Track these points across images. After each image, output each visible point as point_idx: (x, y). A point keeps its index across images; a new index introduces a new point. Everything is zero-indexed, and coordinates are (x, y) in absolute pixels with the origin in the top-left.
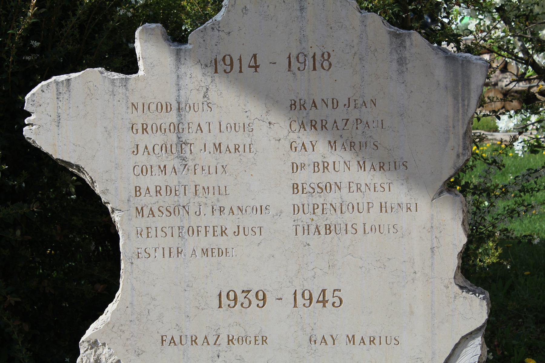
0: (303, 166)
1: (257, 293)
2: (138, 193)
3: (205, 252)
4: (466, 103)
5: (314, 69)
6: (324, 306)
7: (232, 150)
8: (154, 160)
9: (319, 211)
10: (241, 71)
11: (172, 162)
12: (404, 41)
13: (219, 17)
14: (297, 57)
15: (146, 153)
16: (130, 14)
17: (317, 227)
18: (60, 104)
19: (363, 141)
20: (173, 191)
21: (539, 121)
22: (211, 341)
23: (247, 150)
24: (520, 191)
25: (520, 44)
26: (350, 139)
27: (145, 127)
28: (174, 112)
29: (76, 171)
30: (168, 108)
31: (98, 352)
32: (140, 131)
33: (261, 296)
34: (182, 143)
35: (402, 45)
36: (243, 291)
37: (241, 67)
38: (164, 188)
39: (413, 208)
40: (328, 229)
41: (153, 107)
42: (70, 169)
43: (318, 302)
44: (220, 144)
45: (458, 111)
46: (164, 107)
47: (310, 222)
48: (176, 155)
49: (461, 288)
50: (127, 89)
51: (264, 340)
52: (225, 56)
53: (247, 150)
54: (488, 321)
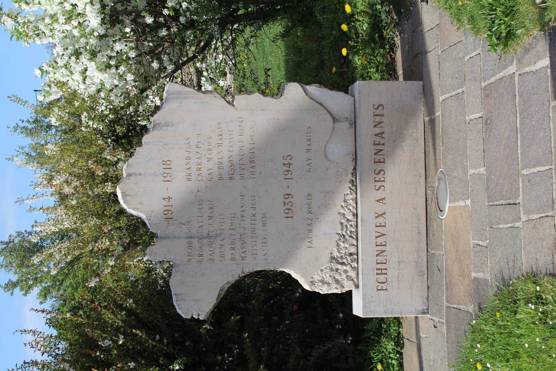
1: (285, 198)
2: (234, 259)
3: (264, 225)
4: (188, 93)
5: (171, 168)
6: (292, 164)
7: (212, 210)
8: (217, 251)
9: (243, 167)
10: (172, 206)
11: (218, 242)
12: (157, 123)
14: (165, 177)
15: (213, 255)
17: (251, 167)
19: (207, 144)
20: (233, 241)
21: (207, 70)
22: (310, 222)
23: (212, 203)
24: (244, 78)
25: (161, 80)
27: (200, 255)
28: (192, 240)
30: (190, 243)
32: (202, 258)
33: (287, 196)
34: (208, 236)
35: (159, 124)
36: (285, 205)
37: (170, 206)
38: (232, 246)
39: (241, 119)
40: (252, 162)
41: (190, 251)
43: (289, 167)
44: (209, 217)
46: (190, 245)
47: (249, 171)
49: (281, 96)
50: (180, 265)
51: (310, 195)
52: (164, 214)
53: (212, 203)
54: (298, 82)
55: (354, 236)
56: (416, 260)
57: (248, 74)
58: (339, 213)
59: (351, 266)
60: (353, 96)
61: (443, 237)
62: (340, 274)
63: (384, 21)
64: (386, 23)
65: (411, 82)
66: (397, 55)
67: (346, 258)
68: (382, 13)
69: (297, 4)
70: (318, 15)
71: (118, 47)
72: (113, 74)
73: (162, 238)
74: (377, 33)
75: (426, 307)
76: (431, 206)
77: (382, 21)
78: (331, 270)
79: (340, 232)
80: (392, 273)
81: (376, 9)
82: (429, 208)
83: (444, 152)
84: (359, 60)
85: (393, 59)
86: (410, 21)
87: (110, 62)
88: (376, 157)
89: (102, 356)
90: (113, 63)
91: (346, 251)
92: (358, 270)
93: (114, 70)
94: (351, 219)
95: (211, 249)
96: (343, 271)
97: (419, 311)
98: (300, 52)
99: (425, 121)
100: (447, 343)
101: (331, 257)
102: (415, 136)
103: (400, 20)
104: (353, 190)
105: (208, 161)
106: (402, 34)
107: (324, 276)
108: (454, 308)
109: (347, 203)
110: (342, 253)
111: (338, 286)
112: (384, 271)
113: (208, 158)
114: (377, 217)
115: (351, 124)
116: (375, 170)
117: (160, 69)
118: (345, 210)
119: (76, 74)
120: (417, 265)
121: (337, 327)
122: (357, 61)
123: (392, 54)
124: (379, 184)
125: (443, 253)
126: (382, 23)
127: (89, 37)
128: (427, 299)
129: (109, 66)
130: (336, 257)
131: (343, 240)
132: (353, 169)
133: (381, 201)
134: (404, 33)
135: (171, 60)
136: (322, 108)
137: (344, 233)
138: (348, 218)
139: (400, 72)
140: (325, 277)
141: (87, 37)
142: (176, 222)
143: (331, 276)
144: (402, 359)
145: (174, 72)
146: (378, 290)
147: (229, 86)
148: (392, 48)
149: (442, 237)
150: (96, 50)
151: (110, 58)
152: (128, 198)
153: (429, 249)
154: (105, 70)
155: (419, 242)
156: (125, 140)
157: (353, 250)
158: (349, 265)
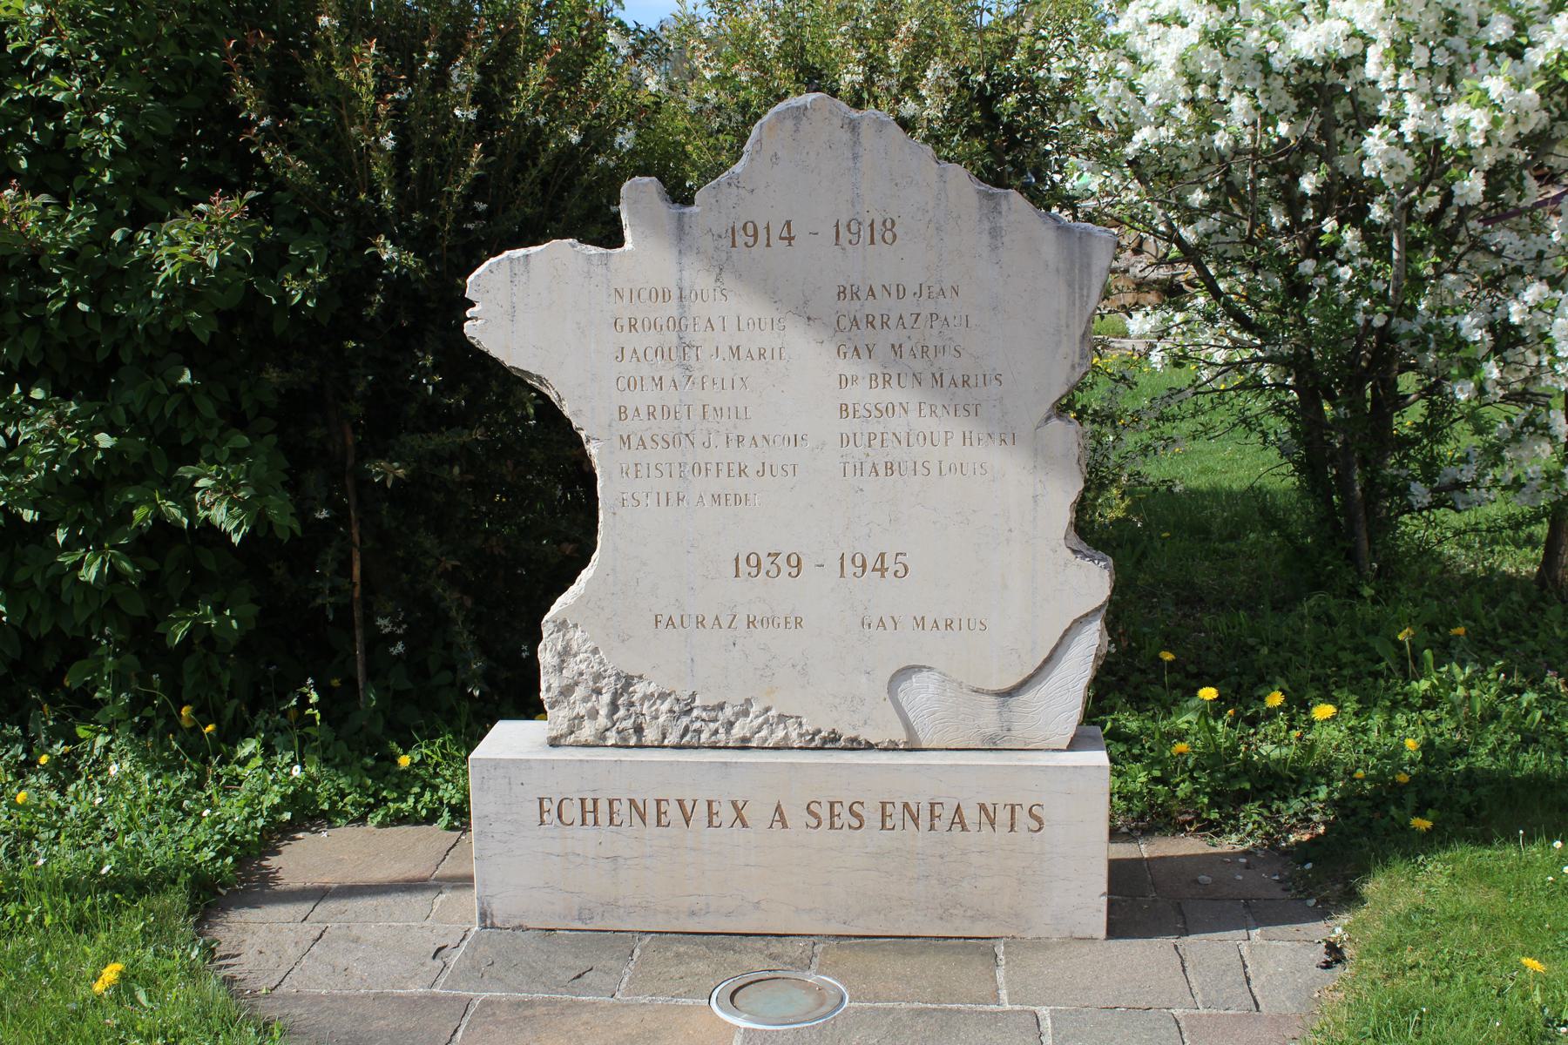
0: (855, 380)
2: (623, 416)
3: (716, 499)
4: (1085, 292)
5: (872, 242)
6: (883, 576)
7: (756, 356)
8: (645, 370)
11: (670, 372)
12: (998, 204)
13: (737, 168)
14: (849, 225)
15: (635, 359)
16: (612, 164)
19: (940, 344)
20: (672, 413)
21: (1186, 322)
22: (725, 622)
24: (1157, 419)
25: (1160, 212)
26: (922, 343)
27: (633, 322)
28: (674, 302)
30: (665, 295)
31: (567, 637)
32: (626, 328)
34: (684, 346)
35: (996, 210)
38: (659, 409)
40: (889, 468)
41: (645, 295)
44: (738, 348)
46: (660, 295)
47: (863, 458)
49: (1075, 552)
51: (798, 623)
54: (1110, 600)
55: (687, 738)
56: (620, 903)
57: (1167, 428)
58: (748, 701)
59: (607, 730)
60: (1073, 745)
61: (660, 999)
62: (586, 700)
63: (1283, 806)
64: (1278, 811)
65: (1104, 908)
67: (630, 716)
68: (1306, 800)
69: (1343, 549)
70: (1312, 602)
71: (1239, 104)
72: (1174, 93)
73: (680, 217)
74: (1253, 786)
75: (498, 922)
76: (761, 952)
77: (1285, 799)
78: (598, 677)
79: (698, 702)
81: (1318, 785)
82: (760, 943)
83: (890, 1019)
84: (1188, 722)
85: (1181, 828)
86: (1277, 892)
87: (1203, 86)
88: (899, 807)
91: (648, 718)
92: (598, 746)
93: (1183, 94)
94: (733, 732)
95: (650, 353)
96: (593, 707)
97: (489, 904)
98: (1233, 537)
99: (997, 941)
100: (377, 997)
101: (632, 678)
102: (955, 912)
103: (1288, 852)
104: (812, 739)
105: (893, 346)
106: (1244, 860)
107: (581, 656)
108: (456, 1031)
109: (778, 724)
110: (642, 705)
111: (555, 692)
112: (590, 817)
113: (900, 346)
114: (734, 804)
115: (992, 739)
116: (862, 804)
117: (1188, 208)
118: (757, 717)
120: (608, 904)
121: (525, 647)
122: (1185, 718)
123: (1196, 825)
124: (824, 813)
125: (618, 995)
126: (1279, 798)
127: (1265, 28)
128: (520, 927)
129: (1193, 82)
131: (676, 708)
133: (777, 817)
134: (1247, 866)
135: (1208, 235)
137: (695, 713)
138: (737, 724)
139: (1145, 849)
140: (578, 659)
141: (1264, 24)
142: (724, 256)
143: (581, 674)
144: (417, 823)
145: (1180, 242)
147: (1136, 384)
148: (1212, 828)
149: (662, 993)
150: (1229, 46)
151: (1215, 86)
152: (789, 124)
153: (649, 937)
154: (1184, 73)
155: (668, 912)
157: (650, 735)
158: (609, 725)
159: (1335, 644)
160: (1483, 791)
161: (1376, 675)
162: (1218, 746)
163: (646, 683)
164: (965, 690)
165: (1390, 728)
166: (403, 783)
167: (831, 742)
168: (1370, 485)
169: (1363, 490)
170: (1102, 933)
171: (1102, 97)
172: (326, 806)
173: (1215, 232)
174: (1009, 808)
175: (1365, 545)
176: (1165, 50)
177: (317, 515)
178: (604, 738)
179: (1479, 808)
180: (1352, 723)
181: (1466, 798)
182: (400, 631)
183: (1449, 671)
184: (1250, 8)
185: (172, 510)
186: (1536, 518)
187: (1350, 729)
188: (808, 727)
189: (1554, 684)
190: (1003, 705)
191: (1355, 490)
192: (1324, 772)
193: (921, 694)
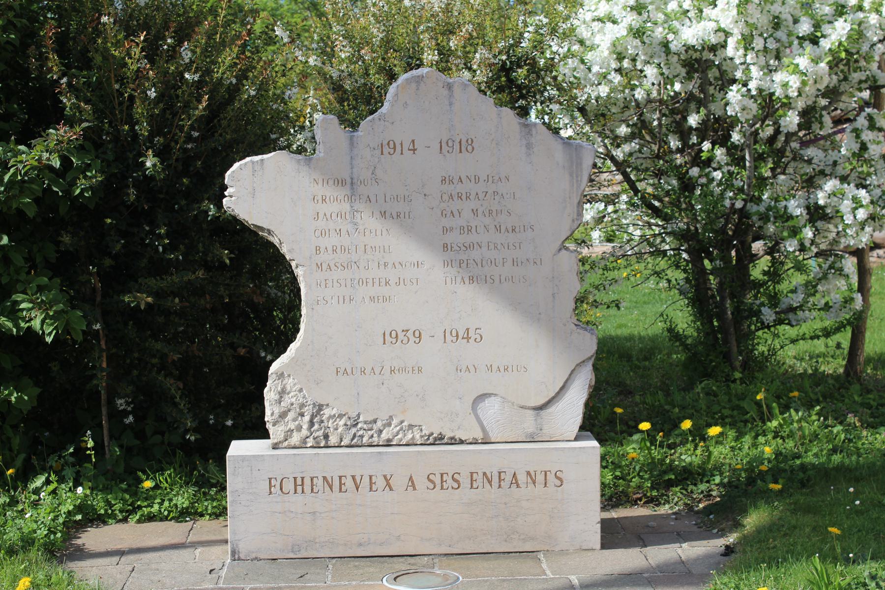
0: (452, 229)
1: (414, 332)
2: (318, 252)
3: (372, 299)
4: (579, 179)
5: (461, 152)
6: (468, 342)
7: (395, 217)
9: (464, 265)
10: (402, 154)
12: (530, 130)
13: (383, 110)
14: (447, 143)
16: (281, 108)
18: (255, 180)
20: (347, 250)
21: (616, 212)
22: (377, 371)
23: (407, 216)
24: (604, 270)
26: (489, 208)
27: (324, 198)
29: (266, 235)
31: (284, 382)
32: (320, 201)
35: (529, 133)
37: (402, 150)
38: (339, 248)
39: (538, 263)
42: (260, 233)
43: (463, 338)
44: (385, 212)
45: (573, 185)
48: (349, 220)
49: (576, 325)
51: (420, 370)
53: (407, 216)
55: (355, 440)
56: (317, 540)
57: (611, 275)
58: (391, 417)
59: (307, 437)
60: (577, 439)
61: (354, 583)
62: (295, 420)
63: (694, 488)
65: (599, 531)
66: (642, 509)
67: (321, 429)
68: (708, 485)
70: (703, 385)
71: (651, 72)
72: (608, 64)
73: (351, 138)
74: (676, 477)
75: (242, 556)
76: (404, 563)
77: (695, 485)
78: (302, 406)
79: (361, 419)
80: (297, 502)
81: (714, 476)
82: (401, 559)
83: (488, 583)
85: (635, 503)
86: (695, 529)
87: (626, 60)
88: (481, 475)
89: (165, 47)
90: (626, 64)
91: (332, 429)
92: (301, 448)
93: (614, 65)
97: (237, 545)
99: (538, 553)
101: (322, 405)
103: (698, 512)
104: (428, 439)
105: (473, 210)
106: (674, 517)
109: (408, 430)
110: (328, 422)
111: (276, 416)
112: (299, 489)
114: (385, 476)
115: (532, 435)
116: (459, 474)
117: (617, 137)
118: (396, 426)
119: (608, 6)
120: (310, 541)
121: (212, 417)
122: (631, 447)
124: (438, 480)
126: (692, 484)
127: (666, 26)
128: (256, 558)
129: (620, 58)
130: (322, 412)
131: (349, 423)
132: (460, 440)
133: (410, 484)
134: (676, 519)
135: (631, 154)
136: (557, 389)
137: (360, 426)
138: (384, 431)
139: (614, 514)
142: (377, 160)
143: (292, 404)
144: (161, 520)
145: (613, 159)
146: (270, 479)
147: (591, 246)
149: (354, 580)
150: (645, 37)
151: (634, 60)
152: (414, 85)
153: (334, 560)
154: (614, 52)
155: (345, 545)
156: (505, 81)
157: (333, 440)
158: (309, 434)
159: (720, 405)
160: (810, 473)
161: (746, 422)
162: (653, 459)
163: (331, 408)
164: (515, 407)
165: (755, 445)
166: (149, 497)
167: (439, 440)
168: (737, 310)
169: (732, 314)
170: (599, 546)
171: (566, 70)
172: (102, 512)
173: (635, 152)
174: (543, 473)
175: (735, 349)
176: (603, 38)
177: (94, 327)
178: (305, 443)
179: (808, 480)
180: (733, 444)
181: (801, 475)
182: (129, 409)
183: (790, 416)
184: (655, 13)
185: (6, 323)
186: (838, 329)
187: (731, 448)
188: (426, 432)
189: (852, 421)
190: (538, 415)
191: (727, 314)
192: (718, 468)
193: (491, 410)
